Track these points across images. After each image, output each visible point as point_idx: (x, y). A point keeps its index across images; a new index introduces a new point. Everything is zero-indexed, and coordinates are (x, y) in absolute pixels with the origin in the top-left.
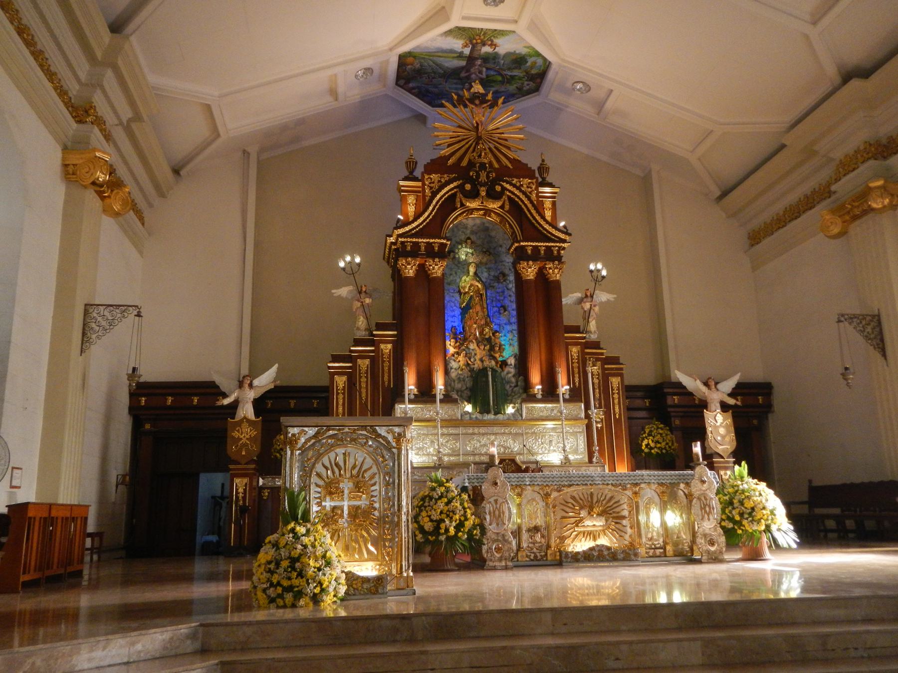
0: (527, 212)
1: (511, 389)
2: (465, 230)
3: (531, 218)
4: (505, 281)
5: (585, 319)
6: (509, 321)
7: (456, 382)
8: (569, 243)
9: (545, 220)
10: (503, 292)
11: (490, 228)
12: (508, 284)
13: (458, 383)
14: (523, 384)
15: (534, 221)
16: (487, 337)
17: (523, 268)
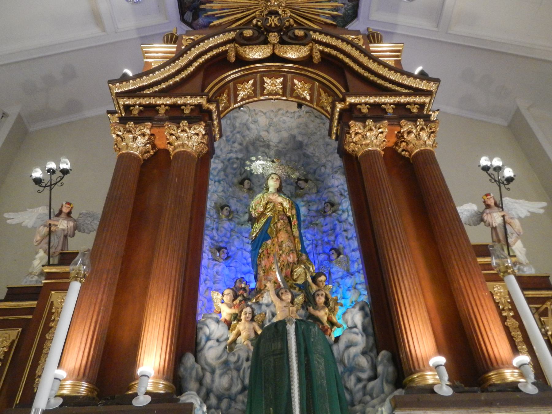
0: (352, 64)
1: (360, 386)
2: (267, 151)
3: (361, 71)
4: (334, 212)
5: (499, 241)
6: (348, 271)
7: (218, 372)
8: (438, 110)
9: (385, 65)
10: (334, 229)
11: (305, 142)
12: (341, 215)
13: (221, 375)
14: (391, 369)
15: (366, 74)
16: (300, 282)
17: (357, 134)
